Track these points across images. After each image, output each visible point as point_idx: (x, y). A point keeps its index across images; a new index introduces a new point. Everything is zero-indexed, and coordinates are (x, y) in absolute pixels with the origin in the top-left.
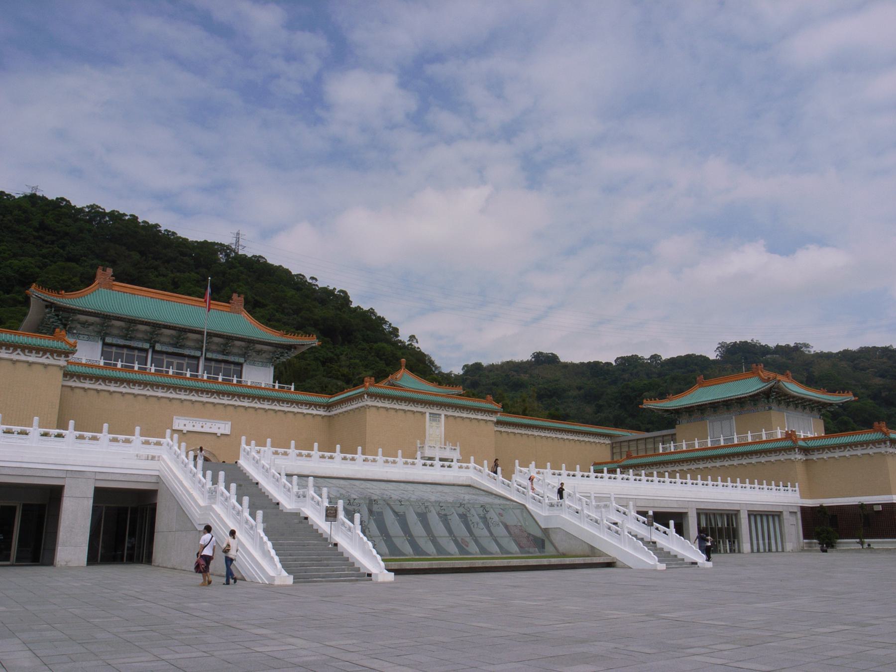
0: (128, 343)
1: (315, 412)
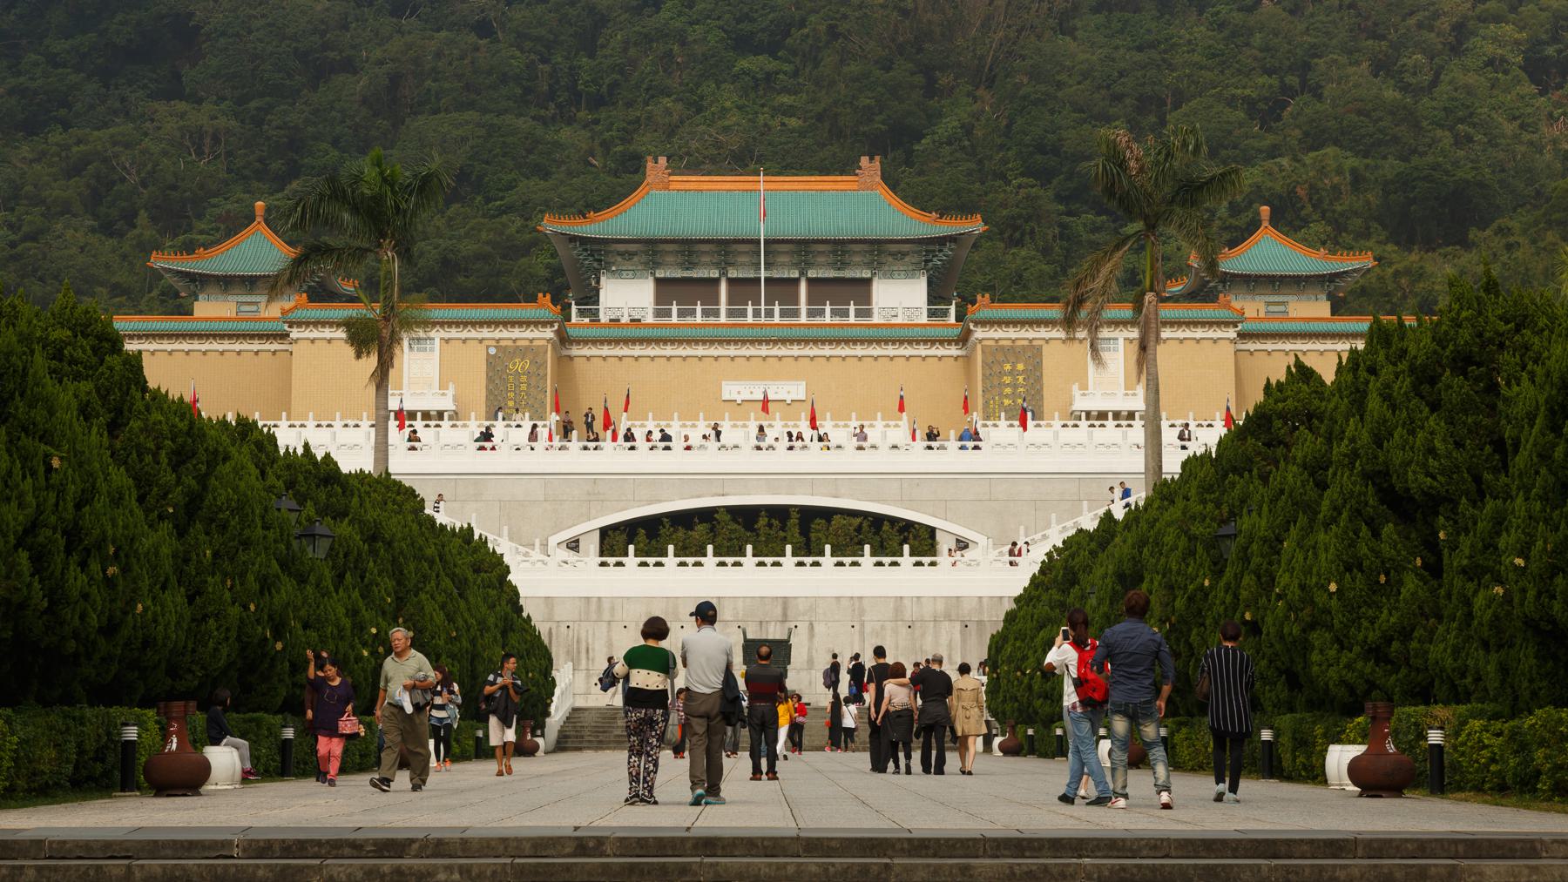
0: (687, 274)
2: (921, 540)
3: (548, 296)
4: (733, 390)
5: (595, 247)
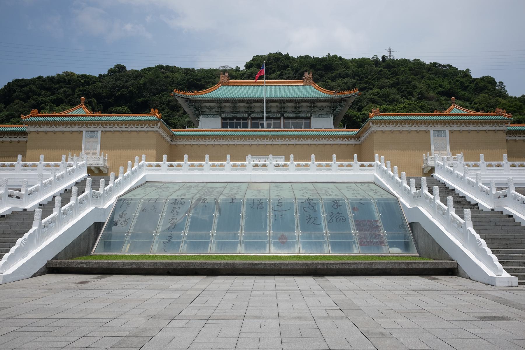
0: (234, 115)
1: (347, 142)
3: (157, 111)
5: (197, 105)
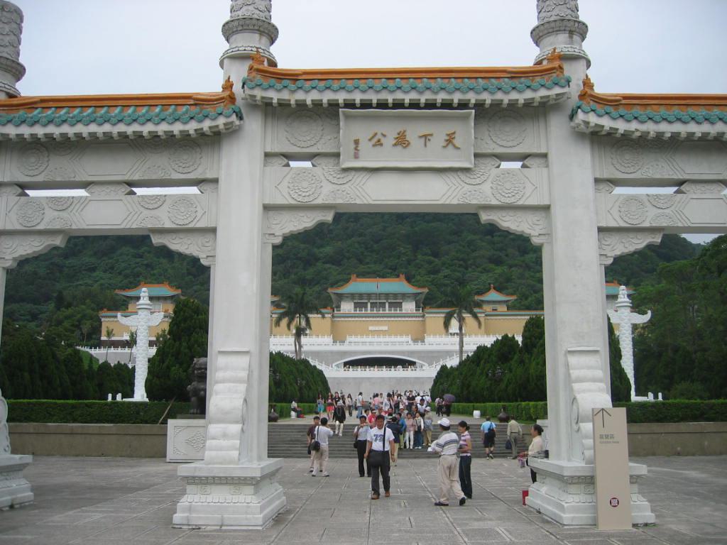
1: (417, 319)
2: (412, 363)
4: (371, 328)
